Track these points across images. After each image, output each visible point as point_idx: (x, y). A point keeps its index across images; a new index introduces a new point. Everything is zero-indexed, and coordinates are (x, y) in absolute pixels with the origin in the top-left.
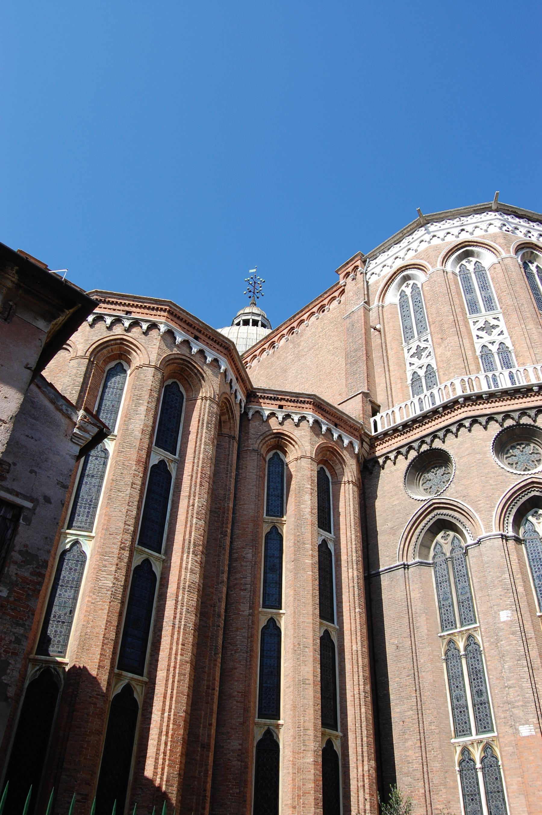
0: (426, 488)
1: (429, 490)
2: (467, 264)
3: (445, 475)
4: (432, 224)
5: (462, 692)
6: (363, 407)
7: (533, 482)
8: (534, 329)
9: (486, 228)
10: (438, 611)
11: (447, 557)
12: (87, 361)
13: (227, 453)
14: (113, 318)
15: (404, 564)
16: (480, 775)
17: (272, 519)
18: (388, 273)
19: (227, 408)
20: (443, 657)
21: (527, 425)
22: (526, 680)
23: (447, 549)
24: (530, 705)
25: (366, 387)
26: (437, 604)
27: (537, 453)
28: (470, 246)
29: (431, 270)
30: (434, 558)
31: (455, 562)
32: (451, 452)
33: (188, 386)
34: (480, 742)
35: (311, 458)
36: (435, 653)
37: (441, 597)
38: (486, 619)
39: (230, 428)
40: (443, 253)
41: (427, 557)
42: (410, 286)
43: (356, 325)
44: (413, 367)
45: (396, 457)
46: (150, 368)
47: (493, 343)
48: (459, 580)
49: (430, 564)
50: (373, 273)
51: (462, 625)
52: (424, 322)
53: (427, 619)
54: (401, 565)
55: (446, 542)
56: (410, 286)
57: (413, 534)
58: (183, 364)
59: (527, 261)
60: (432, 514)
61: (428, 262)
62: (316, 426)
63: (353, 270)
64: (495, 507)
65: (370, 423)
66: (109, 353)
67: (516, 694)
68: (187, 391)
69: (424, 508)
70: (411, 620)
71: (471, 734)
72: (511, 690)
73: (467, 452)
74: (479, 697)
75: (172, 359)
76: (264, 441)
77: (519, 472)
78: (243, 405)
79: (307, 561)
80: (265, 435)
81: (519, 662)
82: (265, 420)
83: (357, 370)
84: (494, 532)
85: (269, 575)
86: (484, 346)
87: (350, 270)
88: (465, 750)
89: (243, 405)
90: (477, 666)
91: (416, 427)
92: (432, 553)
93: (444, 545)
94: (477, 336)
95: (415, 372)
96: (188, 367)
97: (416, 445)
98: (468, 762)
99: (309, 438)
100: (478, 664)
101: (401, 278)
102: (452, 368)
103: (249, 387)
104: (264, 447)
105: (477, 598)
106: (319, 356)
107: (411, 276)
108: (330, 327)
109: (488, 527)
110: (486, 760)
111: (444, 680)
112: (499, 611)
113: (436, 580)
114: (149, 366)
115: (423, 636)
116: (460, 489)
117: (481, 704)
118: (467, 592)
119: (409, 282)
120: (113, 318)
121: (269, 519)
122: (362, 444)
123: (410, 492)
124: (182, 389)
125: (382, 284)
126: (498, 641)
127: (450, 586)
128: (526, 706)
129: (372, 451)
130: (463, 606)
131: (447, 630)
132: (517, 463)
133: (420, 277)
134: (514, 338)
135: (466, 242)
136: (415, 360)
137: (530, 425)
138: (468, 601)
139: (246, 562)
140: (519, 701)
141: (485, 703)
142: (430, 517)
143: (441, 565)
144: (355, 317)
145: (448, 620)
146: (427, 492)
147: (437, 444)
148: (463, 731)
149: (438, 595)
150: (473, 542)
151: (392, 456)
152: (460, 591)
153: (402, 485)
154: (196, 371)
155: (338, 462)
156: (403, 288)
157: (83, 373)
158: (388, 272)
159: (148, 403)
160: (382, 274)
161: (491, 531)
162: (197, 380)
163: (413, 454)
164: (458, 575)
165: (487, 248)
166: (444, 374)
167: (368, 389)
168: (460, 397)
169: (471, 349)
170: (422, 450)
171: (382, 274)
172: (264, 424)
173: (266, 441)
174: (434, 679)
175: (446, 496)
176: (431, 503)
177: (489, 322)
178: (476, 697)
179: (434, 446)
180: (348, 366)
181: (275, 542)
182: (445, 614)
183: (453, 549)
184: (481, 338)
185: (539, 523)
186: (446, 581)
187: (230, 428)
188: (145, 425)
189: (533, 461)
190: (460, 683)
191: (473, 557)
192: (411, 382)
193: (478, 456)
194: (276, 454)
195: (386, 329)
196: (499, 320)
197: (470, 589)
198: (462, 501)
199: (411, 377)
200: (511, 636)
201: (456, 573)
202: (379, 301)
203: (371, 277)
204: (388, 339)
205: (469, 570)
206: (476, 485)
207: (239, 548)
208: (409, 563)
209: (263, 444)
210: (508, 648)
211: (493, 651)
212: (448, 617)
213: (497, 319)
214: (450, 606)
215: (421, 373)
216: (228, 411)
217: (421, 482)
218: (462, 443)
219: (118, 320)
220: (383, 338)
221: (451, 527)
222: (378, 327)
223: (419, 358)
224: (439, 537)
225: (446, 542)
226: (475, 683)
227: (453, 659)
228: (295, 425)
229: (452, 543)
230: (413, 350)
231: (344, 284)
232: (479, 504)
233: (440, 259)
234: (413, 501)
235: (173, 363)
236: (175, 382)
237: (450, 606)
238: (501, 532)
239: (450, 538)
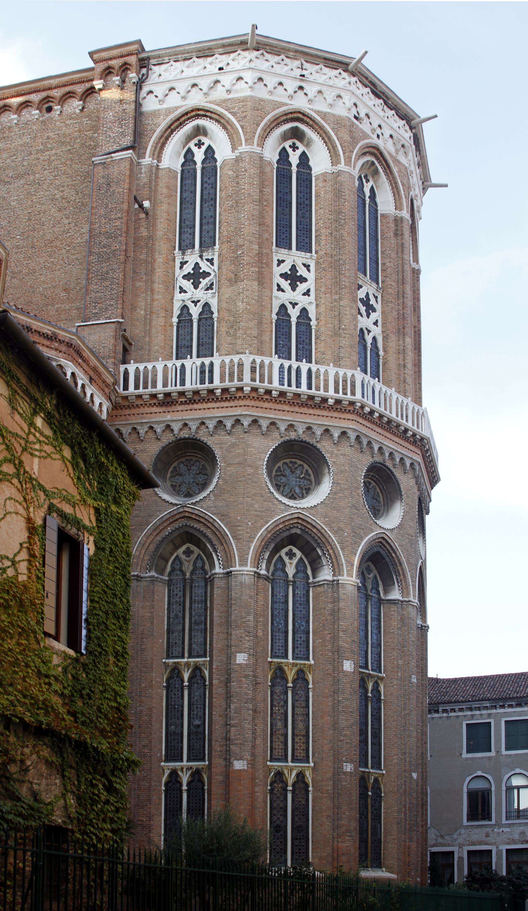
3: (201, 475)
9: (332, 102)
16: (185, 796)
18: (177, 108)
26: (166, 626)
30: (170, 574)
32: (218, 453)
34: (189, 768)
38: (220, 656)
42: (204, 148)
47: (294, 305)
50: (151, 92)
64: (255, 538)
67: (237, 733)
71: (181, 760)
72: (232, 728)
83: (107, 273)
84: (249, 568)
88: (174, 773)
91: (181, 402)
93: (184, 562)
94: (278, 285)
98: (174, 784)
101: (194, 127)
105: (215, 633)
107: (209, 132)
108: (58, 151)
110: (192, 784)
112: (237, 652)
115: (147, 660)
116: (221, 504)
118: (202, 622)
119: (204, 139)
125: (164, 124)
135: (300, 113)
140: (238, 739)
146: (174, 490)
148: (174, 756)
150: (221, 571)
156: (192, 145)
161: (246, 565)
166: (227, 332)
175: (202, 507)
177: (298, 268)
184: (283, 291)
191: (218, 587)
196: (309, 270)
197: (206, 619)
198: (219, 520)
200: (243, 679)
202: (154, 154)
205: (209, 599)
206: (240, 506)
210: (238, 690)
211: (220, 689)
213: (307, 267)
215: (195, 311)
221: (199, 544)
222: (146, 204)
231: (101, 86)
238: (255, 569)
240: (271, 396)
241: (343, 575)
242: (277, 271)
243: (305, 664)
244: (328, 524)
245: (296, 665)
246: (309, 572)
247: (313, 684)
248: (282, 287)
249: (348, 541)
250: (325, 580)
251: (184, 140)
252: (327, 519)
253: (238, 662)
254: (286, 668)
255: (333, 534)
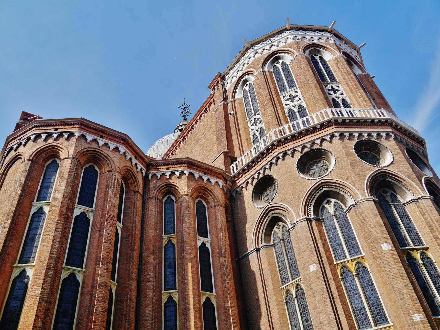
0: (265, 200)
1: (267, 201)
2: (277, 65)
4: (255, 46)
5: (297, 321)
6: (224, 160)
7: (323, 183)
8: (316, 92)
10: (279, 274)
11: (280, 239)
12: (30, 162)
13: (133, 201)
14: (47, 134)
15: (256, 248)
17: (168, 236)
19: (131, 175)
20: (285, 301)
21: (316, 149)
22: (329, 306)
23: (280, 234)
24: (332, 322)
25: (227, 149)
26: (278, 269)
27: (326, 165)
28: (277, 53)
29: (256, 72)
31: (285, 241)
33: (100, 166)
35: (188, 195)
36: (279, 300)
37: (280, 264)
38: (303, 272)
39: (135, 187)
40: (262, 61)
41: (269, 241)
43: (220, 114)
44: (253, 131)
45: (247, 186)
46: (69, 159)
47: (295, 106)
48: (288, 252)
49: (271, 245)
50: (228, 83)
51: (293, 279)
52: (256, 104)
53: (272, 279)
54: (255, 249)
55: (279, 230)
56: (248, 85)
57: (260, 229)
58: (94, 153)
59: (313, 55)
60: (269, 215)
61: (254, 69)
62: (191, 176)
63: (217, 84)
65: (230, 169)
66: (46, 155)
67: (324, 316)
68: (100, 169)
69: (264, 212)
70: (263, 282)
72: (321, 314)
73: (283, 173)
74: (306, 322)
75: (85, 151)
76: (159, 191)
77: (315, 179)
78: (144, 172)
79: (188, 257)
80: (159, 187)
81: (324, 296)
82: (159, 178)
84: (302, 218)
85: (168, 270)
86: (290, 110)
87: (215, 84)
89: (144, 172)
90: (303, 303)
92: (272, 239)
94: (286, 104)
95: (255, 134)
96: (98, 155)
97: (255, 176)
99: (186, 183)
100: (304, 302)
102: (271, 126)
103: (147, 161)
104: (160, 194)
106: (207, 138)
107: (247, 79)
109: (298, 216)
111: (286, 316)
112: (309, 265)
113: (276, 255)
114: (69, 157)
117: (308, 327)
120: (47, 134)
121: (166, 236)
122: (226, 182)
123: (255, 204)
124: (97, 168)
126: (311, 284)
127: (284, 256)
128: (330, 323)
129: (233, 185)
130: (292, 267)
131: (285, 284)
132: (314, 174)
133: (251, 78)
134: (306, 100)
136: (254, 127)
137: (318, 149)
138: (295, 263)
139: (150, 264)
141: (310, 326)
142: (268, 217)
143: (278, 245)
144: (219, 110)
145: (285, 277)
147: (268, 172)
149: (278, 263)
151: (244, 185)
152: (289, 258)
153: (251, 201)
154: (103, 156)
155: (209, 195)
156: (245, 87)
157: (27, 170)
158: (235, 80)
159: (67, 179)
160: (232, 82)
161: (300, 217)
162: (105, 161)
163: (255, 181)
164: (287, 248)
165: (287, 53)
167: (228, 149)
168: (275, 141)
169: (282, 112)
170: (259, 178)
171: (232, 82)
172: (158, 181)
173: (161, 191)
174: (280, 316)
175: (274, 202)
176: (267, 208)
178: (305, 323)
179: (265, 174)
180: (218, 139)
181: (171, 249)
182: (283, 274)
183: (283, 233)
184: (288, 105)
185: (330, 207)
186: (282, 254)
187: (135, 187)
188: (65, 192)
189: (323, 170)
190: (295, 316)
192: (253, 140)
193: (289, 174)
194: (200, 201)
195: (237, 113)
198: (283, 203)
199: (253, 137)
200: (317, 280)
201: (287, 248)
202: (232, 98)
203: (227, 85)
204: (239, 119)
207: (146, 257)
208: (259, 247)
209: (159, 192)
210: (316, 288)
211: (309, 292)
212: (285, 275)
214: (285, 269)
216: (132, 177)
217: (263, 197)
218: (280, 169)
219: (50, 135)
220: (235, 118)
222: (232, 113)
223: (256, 125)
224: (275, 229)
225: (279, 230)
226: (303, 314)
227: (290, 301)
228: (178, 178)
229: (283, 230)
230: (253, 122)
232: (292, 203)
233: (260, 65)
234: (258, 209)
235: (87, 154)
236: (92, 165)
237: (285, 269)
239: (281, 227)
240: (289, 140)
241: (359, 198)
242: (282, 100)
243: (359, 258)
244: (341, 178)
245: (354, 260)
246: (343, 206)
247: (370, 268)
248: (287, 104)
249: (355, 180)
250: (351, 205)
251: (241, 88)
252: (338, 176)
253: (311, 271)
254: (348, 265)
255: (345, 181)
